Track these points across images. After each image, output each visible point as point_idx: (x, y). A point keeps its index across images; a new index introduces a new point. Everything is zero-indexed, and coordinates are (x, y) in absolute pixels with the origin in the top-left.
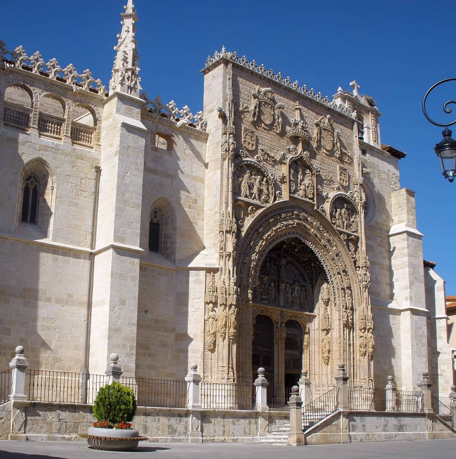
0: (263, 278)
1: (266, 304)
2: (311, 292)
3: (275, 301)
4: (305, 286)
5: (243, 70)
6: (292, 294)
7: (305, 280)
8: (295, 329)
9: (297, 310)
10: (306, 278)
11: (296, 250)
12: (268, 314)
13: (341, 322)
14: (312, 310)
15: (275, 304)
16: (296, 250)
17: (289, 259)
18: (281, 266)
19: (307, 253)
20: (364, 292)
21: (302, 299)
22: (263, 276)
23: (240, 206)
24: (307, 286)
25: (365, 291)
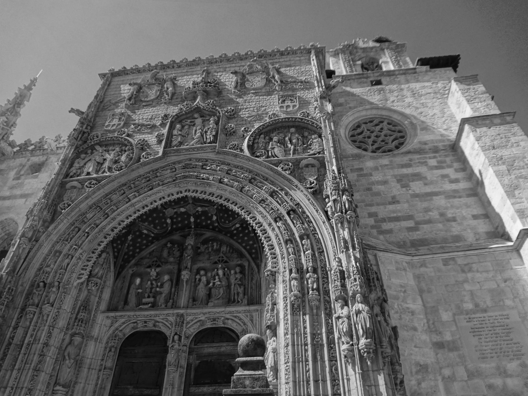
0: (149, 273)
1: (146, 310)
2: (256, 270)
3: (172, 302)
4: (242, 266)
5: (127, 74)
6: (208, 283)
7: (241, 256)
8: (225, 344)
9: (214, 306)
10: (246, 253)
11: (215, 218)
12: (150, 326)
13: (288, 301)
14: (255, 300)
15: (166, 306)
16: (215, 218)
17: (208, 234)
18: (187, 247)
19: (236, 216)
20: (341, 231)
21: (232, 287)
22: (149, 270)
23: (75, 187)
24: (246, 264)
25: (344, 230)
